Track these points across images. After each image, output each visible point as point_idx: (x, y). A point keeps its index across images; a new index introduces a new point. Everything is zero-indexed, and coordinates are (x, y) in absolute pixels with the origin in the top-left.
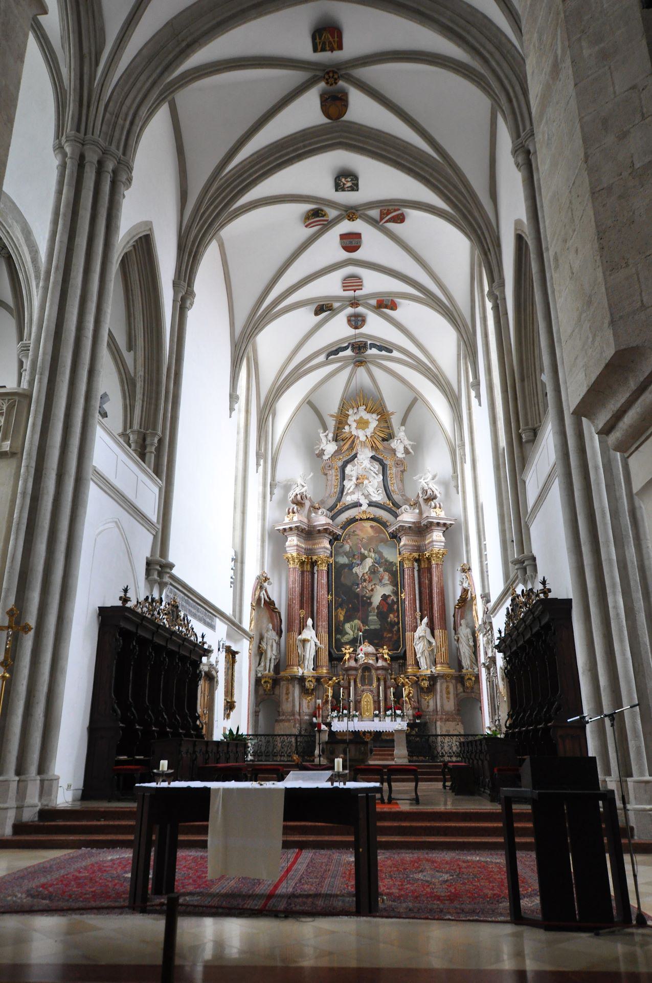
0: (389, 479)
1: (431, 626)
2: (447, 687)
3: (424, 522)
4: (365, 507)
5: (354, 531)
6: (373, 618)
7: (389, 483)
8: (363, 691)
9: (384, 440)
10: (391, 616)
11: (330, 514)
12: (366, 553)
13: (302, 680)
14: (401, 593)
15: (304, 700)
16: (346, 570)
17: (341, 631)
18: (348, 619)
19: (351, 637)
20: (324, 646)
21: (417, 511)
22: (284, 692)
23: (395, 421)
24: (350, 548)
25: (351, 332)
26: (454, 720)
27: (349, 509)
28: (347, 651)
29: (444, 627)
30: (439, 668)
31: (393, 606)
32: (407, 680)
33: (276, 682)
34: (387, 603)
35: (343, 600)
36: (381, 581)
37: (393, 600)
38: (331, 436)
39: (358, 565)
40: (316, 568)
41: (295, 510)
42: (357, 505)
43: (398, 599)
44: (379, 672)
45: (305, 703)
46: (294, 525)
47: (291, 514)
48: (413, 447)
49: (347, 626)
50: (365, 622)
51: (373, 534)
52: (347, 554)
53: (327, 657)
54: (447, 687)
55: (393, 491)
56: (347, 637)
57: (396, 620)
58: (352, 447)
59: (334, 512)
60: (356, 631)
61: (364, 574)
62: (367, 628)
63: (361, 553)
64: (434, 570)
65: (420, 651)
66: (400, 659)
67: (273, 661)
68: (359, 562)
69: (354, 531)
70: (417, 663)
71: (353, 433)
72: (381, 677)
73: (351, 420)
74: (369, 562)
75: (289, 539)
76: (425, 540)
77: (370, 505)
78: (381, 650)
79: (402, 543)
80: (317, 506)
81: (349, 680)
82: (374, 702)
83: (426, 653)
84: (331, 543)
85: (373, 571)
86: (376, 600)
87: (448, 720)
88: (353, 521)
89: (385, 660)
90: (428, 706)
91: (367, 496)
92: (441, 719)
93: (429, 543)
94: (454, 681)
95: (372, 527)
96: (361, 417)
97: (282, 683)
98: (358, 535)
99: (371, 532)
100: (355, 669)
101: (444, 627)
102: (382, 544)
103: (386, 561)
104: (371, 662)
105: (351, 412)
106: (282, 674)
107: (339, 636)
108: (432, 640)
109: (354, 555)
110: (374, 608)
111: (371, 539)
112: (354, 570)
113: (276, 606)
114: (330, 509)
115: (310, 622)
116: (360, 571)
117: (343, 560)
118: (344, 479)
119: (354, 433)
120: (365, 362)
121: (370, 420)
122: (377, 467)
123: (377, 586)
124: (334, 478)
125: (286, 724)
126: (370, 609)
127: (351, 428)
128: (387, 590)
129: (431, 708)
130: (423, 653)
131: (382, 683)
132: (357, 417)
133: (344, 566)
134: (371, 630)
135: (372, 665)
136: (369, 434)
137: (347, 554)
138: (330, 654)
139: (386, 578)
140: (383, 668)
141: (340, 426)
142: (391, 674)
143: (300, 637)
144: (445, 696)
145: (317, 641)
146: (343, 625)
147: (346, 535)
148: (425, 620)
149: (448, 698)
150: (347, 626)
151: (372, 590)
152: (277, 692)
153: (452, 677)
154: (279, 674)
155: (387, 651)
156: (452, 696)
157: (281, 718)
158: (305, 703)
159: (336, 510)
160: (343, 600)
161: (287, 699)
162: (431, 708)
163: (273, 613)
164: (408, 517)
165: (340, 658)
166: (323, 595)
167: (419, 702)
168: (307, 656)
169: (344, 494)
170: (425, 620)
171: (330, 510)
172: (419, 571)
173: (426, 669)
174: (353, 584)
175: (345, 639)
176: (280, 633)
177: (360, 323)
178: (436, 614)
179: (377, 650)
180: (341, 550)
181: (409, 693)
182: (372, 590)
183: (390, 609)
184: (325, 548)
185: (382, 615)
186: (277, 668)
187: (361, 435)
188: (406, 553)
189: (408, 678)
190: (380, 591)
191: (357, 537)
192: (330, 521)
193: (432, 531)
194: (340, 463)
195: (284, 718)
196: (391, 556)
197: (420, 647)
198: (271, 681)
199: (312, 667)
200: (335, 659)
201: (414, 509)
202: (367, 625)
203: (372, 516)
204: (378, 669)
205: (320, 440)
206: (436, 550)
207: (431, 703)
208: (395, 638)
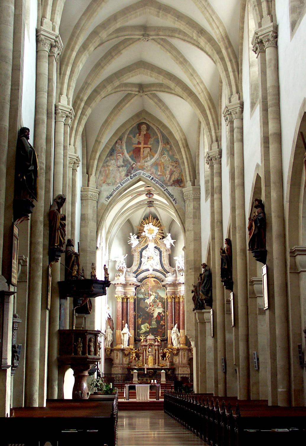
0: (162, 258)
1: (179, 328)
2: (184, 354)
3: (177, 282)
4: (151, 271)
5: (146, 283)
6: (154, 322)
7: (163, 260)
8: (149, 355)
9: (161, 239)
10: (162, 322)
11: (135, 275)
12: (151, 293)
13: (123, 350)
14: (167, 312)
15: (124, 358)
16: (142, 301)
17: (140, 328)
18: (143, 323)
19: (144, 331)
20: (132, 336)
21: (175, 275)
22: (116, 355)
23: (166, 229)
24: (144, 290)
25: (147, 198)
26: (186, 367)
27: (144, 272)
28: (142, 338)
29: (184, 329)
30: (181, 346)
31: (163, 318)
32: (167, 351)
33: (112, 350)
34: (160, 316)
35: (141, 315)
36: (157, 306)
37: (163, 315)
38: (136, 236)
39: (148, 298)
40: (129, 300)
41: (120, 275)
42: (148, 270)
43: (165, 314)
44: (156, 347)
45: (124, 359)
46: (119, 283)
47: (118, 276)
48: (174, 243)
49: (142, 326)
50: (150, 324)
51: (154, 284)
52: (142, 293)
53: (133, 340)
54: (184, 354)
55: (164, 264)
56: (142, 331)
57: (164, 324)
58: (146, 242)
59: (137, 273)
60: (146, 328)
61: (150, 304)
62: (151, 327)
63: (149, 293)
64: (181, 303)
65: (174, 338)
66: (165, 340)
67: (110, 342)
68: (148, 297)
69: (146, 283)
70: (172, 343)
71: (146, 236)
72: (157, 350)
73: (145, 229)
74: (152, 297)
75: (117, 288)
76: (177, 289)
77: (153, 271)
78: (157, 338)
79: (167, 291)
80: (129, 271)
81: (143, 350)
82: (154, 359)
83: (176, 339)
84: (136, 289)
85: (154, 302)
86: (155, 315)
87: (184, 367)
88: (146, 278)
89: (158, 342)
90: (176, 361)
91: (152, 267)
92: (181, 366)
93: (179, 291)
94: (187, 351)
95: (154, 281)
96: (150, 228)
97: (115, 351)
98: (148, 285)
99: (154, 283)
100: (146, 346)
101: (184, 329)
102: (159, 289)
103: (160, 297)
104: (153, 343)
105: (145, 226)
106: (115, 347)
107: (138, 331)
108: (179, 334)
109: (146, 294)
110: (154, 318)
111: (153, 287)
112: (146, 301)
113: (111, 317)
114: (134, 273)
115: (126, 325)
116: (149, 301)
117: (141, 296)
118: (142, 258)
119: (147, 235)
120: (153, 206)
121: (154, 229)
122: (158, 252)
123: (156, 309)
124: (137, 256)
125: (117, 368)
126: (152, 319)
127: (145, 234)
128: (160, 310)
129: (177, 362)
130: (174, 339)
131: (157, 351)
132: (148, 228)
133: (141, 299)
134: (153, 328)
135: (153, 344)
136: (154, 237)
137: (142, 293)
138: (135, 338)
139: (160, 304)
140: (158, 346)
141: (140, 232)
142: (161, 348)
143: (122, 332)
144: (183, 357)
145: (129, 333)
146: (141, 325)
147: (142, 284)
148: (176, 325)
149: (184, 358)
150: (142, 326)
151: (154, 310)
152: (112, 354)
153: (186, 349)
154: (113, 347)
155: (160, 338)
156: (186, 357)
157: (114, 366)
158: (124, 359)
159: (138, 273)
160: (141, 315)
161: (117, 358)
162: (177, 362)
163: (110, 321)
164: (169, 279)
165: (140, 340)
166: (131, 313)
167: (172, 359)
168: (125, 340)
169: (142, 265)
170: (176, 325)
171: (134, 273)
172: (174, 302)
173: (176, 345)
174: (145, 307)
175: (142, 332)
176: (113, 330)
177: (151, 196)
178: (181, 323)
179: (155, 337)
180: (140, 291)
181: (168, 356)
182: (154, 310)
183: (162, 320)
184: (134, 292)
185: (158, 322)
186: (112, 345)
187: (150, 237)
188: (169, 295)
189: (168, 350)
190: (157, 311)
191: (147, 285)
192: (135, 279)
193: (181, 286)
194: (140, 250)
195: (115, 366)
196: (163, 295)
197: (174, 336)
198: (110, 351)
199: (127, 344)
200: (137, 340)
201: (173, 274)
202: (151, 326)
203: (154, 276)
204: (156, 346)
205: (130, 238)
206: (182, 295)
207: (177, 360)
208: (163, 331)
